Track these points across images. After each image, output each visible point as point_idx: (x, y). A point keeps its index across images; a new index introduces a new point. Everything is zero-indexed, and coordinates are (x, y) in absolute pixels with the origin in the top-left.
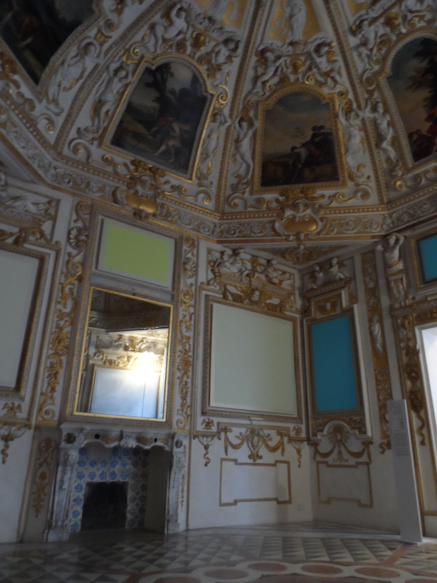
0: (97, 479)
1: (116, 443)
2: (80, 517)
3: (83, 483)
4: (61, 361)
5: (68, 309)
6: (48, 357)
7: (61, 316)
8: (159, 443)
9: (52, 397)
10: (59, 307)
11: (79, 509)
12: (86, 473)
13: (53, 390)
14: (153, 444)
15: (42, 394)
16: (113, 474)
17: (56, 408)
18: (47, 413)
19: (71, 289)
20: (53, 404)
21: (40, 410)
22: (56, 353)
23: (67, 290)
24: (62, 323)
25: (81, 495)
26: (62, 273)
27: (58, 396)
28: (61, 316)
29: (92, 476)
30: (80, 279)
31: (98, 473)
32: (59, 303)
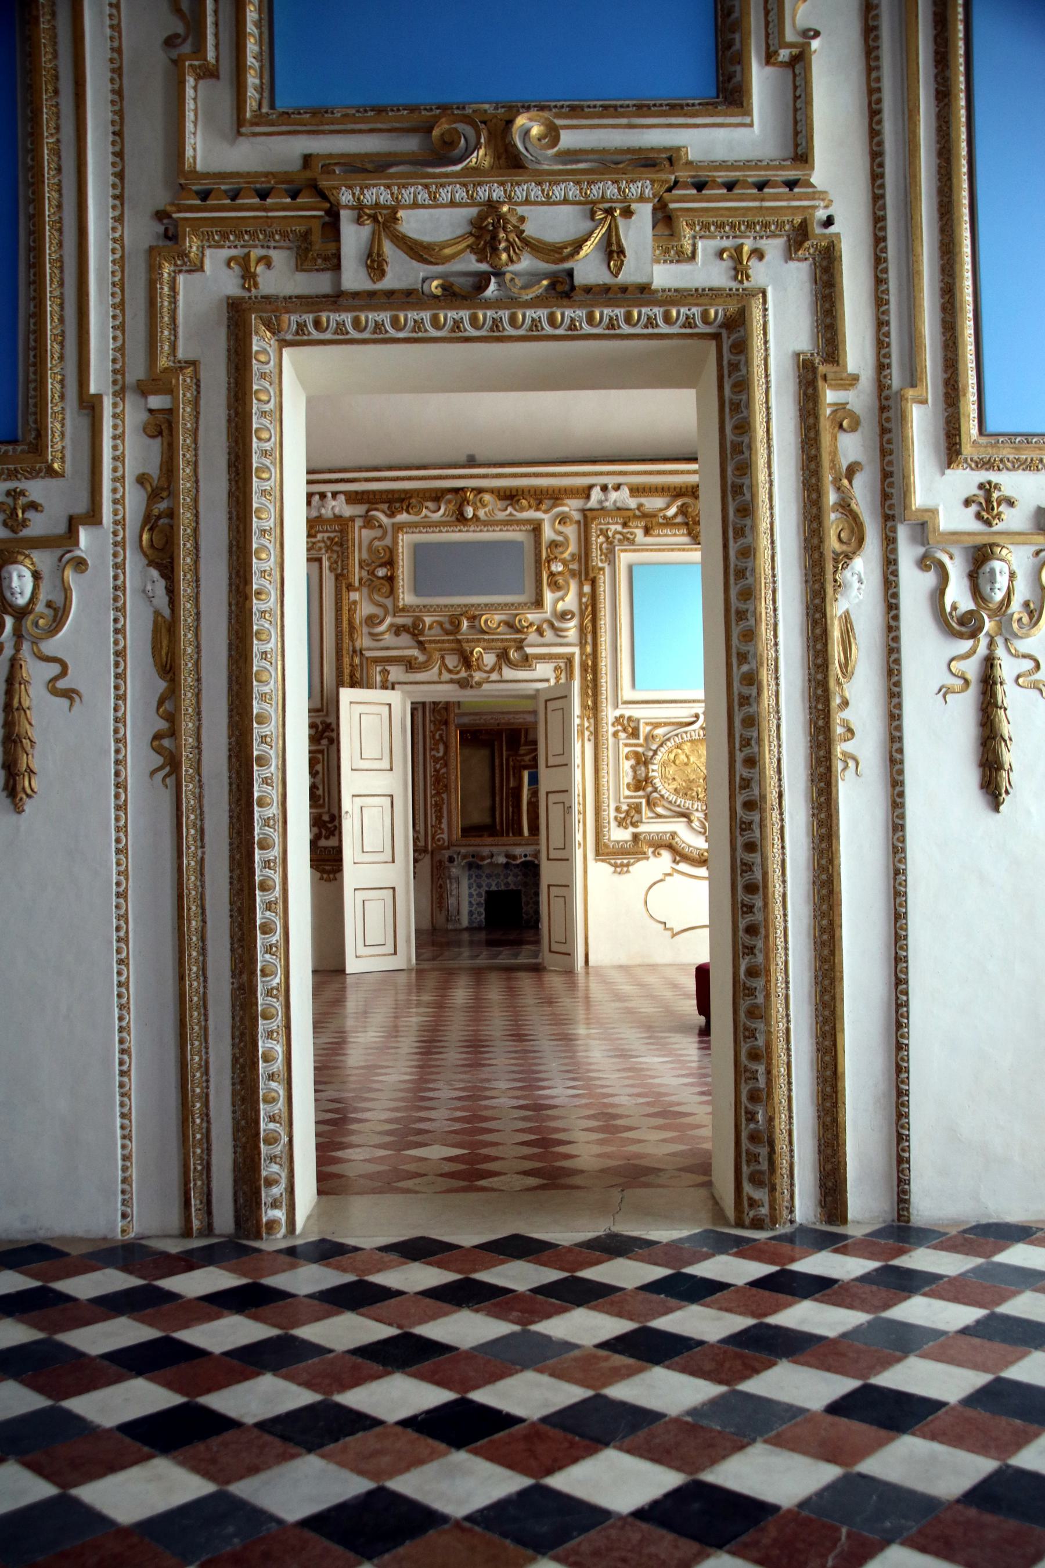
0: (494, 888)
1: (489, 861)
2: (483, 916)
3: (483, 891)
4: (443, 799)
5: (441, 754)
6: (432, 797)
7: (436, 760)
8: (528, 858)
9: (440, 828)
10: (433, 753)
11: (482, 910)
12: (484, 885)
13: (440, 823)
14: (523, 859)
15: (432, 826)
16: (507, 884)
17: (445, 836)
18: (439, 840)
19: (441, 735)
20: (442, 833)
21: (433, 838)
22: (438, 793)
23: (437, 737)
24: (438, 766)
25: (482, 900)
26: (431, 721)
27: (444, 826)
28: (436, 760)
29: (489, 885)
30: (446, 723)
31: (494, 884)
32: (432, 749)
